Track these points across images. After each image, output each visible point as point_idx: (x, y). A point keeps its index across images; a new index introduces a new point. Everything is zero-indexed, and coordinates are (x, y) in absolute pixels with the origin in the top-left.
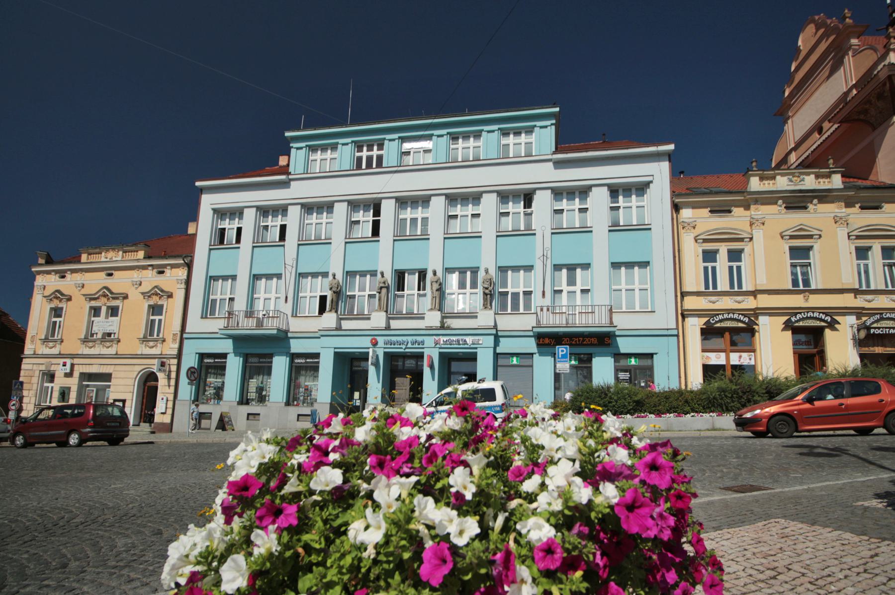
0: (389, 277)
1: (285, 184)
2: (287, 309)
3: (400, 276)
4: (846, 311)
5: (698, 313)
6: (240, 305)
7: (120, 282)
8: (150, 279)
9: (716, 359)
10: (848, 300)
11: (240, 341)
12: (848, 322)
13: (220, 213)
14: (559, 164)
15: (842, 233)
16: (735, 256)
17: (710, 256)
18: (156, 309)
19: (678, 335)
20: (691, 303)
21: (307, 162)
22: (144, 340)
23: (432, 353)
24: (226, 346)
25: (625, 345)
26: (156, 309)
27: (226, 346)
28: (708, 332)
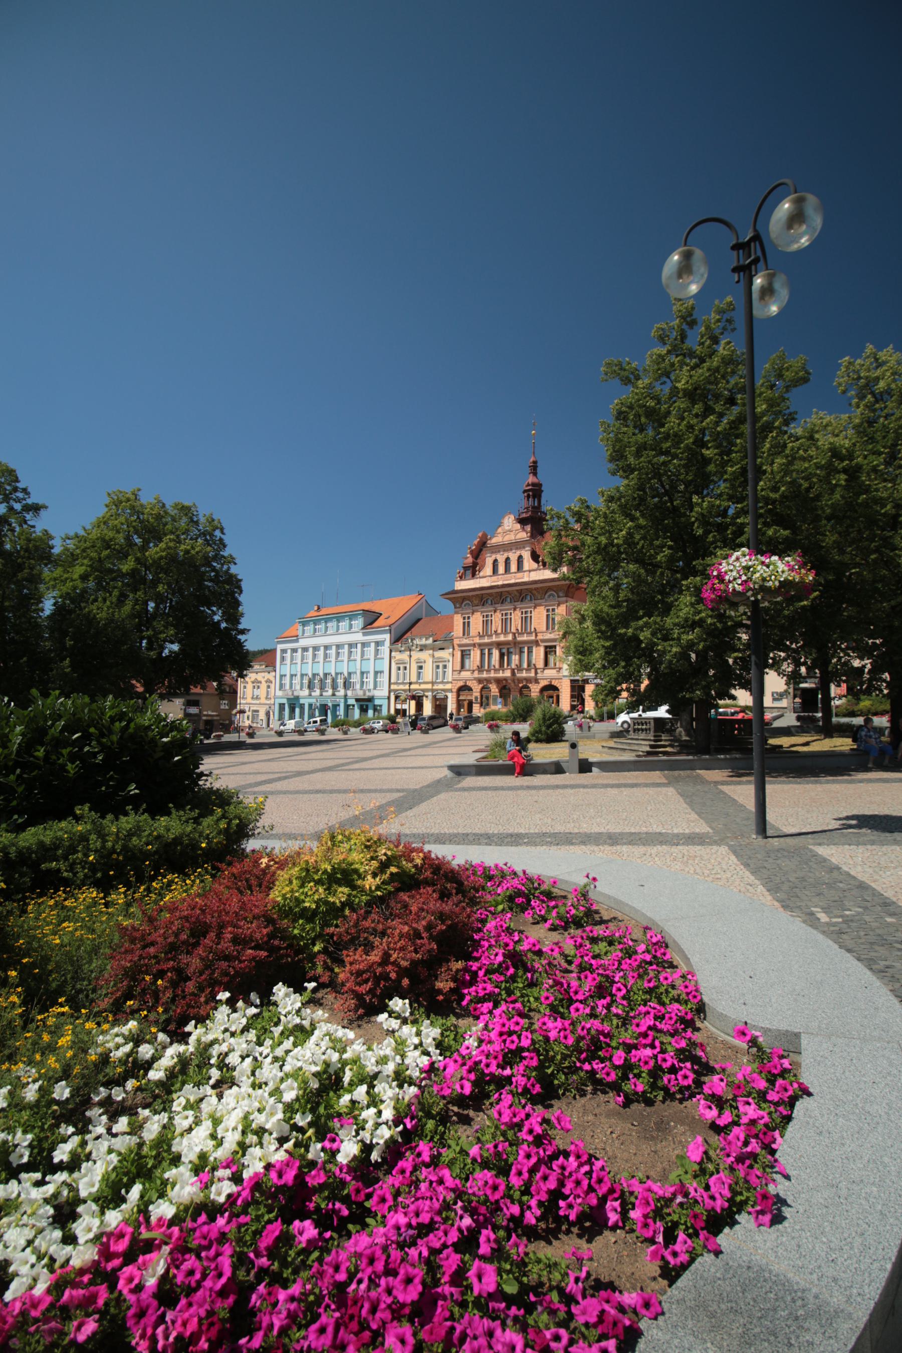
0: (322, 675)
1: (297, 641)
2: (298, 687)
3: (326, 675)
4: (427, 690)
5: (395, 691)
6: (288, 687)
7: (260, 677)
8: (266, 675)
9: (399, 707)
10: (429, 686)
11: (288, 699)
12: (429, 694)
13: (284, 651)
14: (365, 634)
15: (431, 660)
16: (405, 668)
17: (399, 669)
18: (269, 687)
19: (389, 698)
20: (393, 687)
21: (304, 631)
22: (267, 698)
23: (330, 704)
24: (284, 701)
25: (377, 702)
26: (269, 687)
27: (284, 701)
28: (397, 697)
